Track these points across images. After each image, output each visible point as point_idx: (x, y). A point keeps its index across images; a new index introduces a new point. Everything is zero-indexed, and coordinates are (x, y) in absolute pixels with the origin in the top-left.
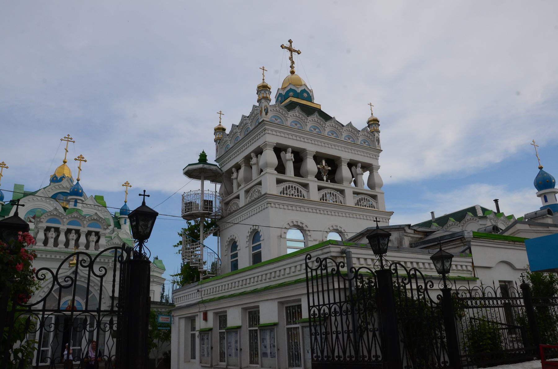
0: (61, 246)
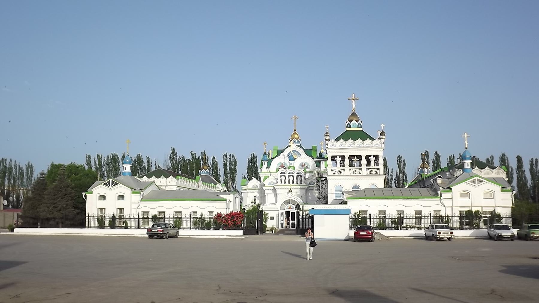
0: (287, 184)
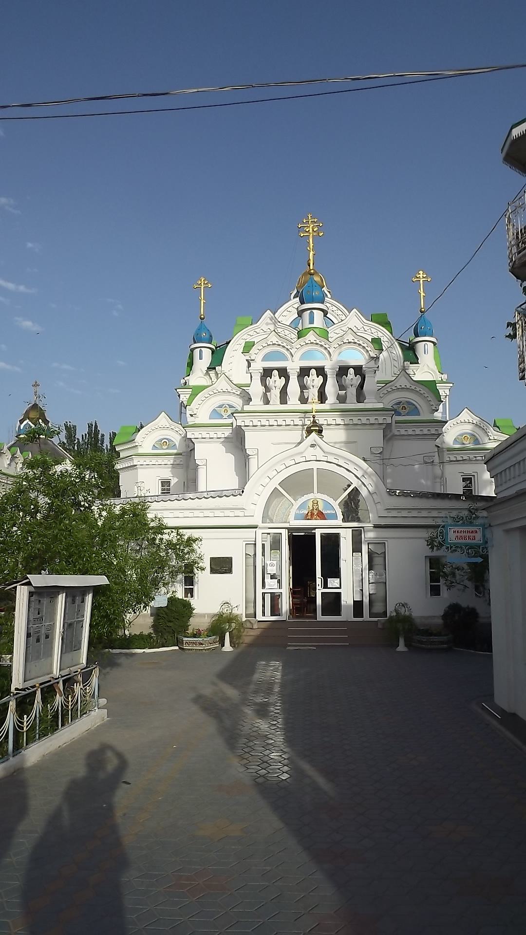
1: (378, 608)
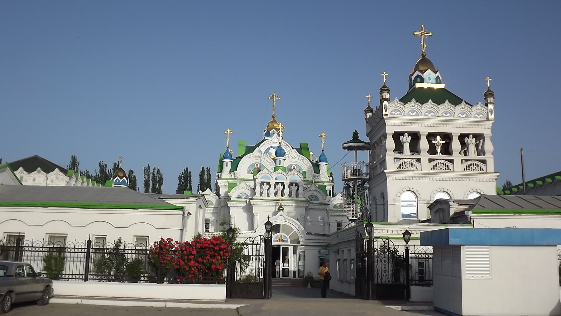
0: (272, 196)
1: (301, 274)
